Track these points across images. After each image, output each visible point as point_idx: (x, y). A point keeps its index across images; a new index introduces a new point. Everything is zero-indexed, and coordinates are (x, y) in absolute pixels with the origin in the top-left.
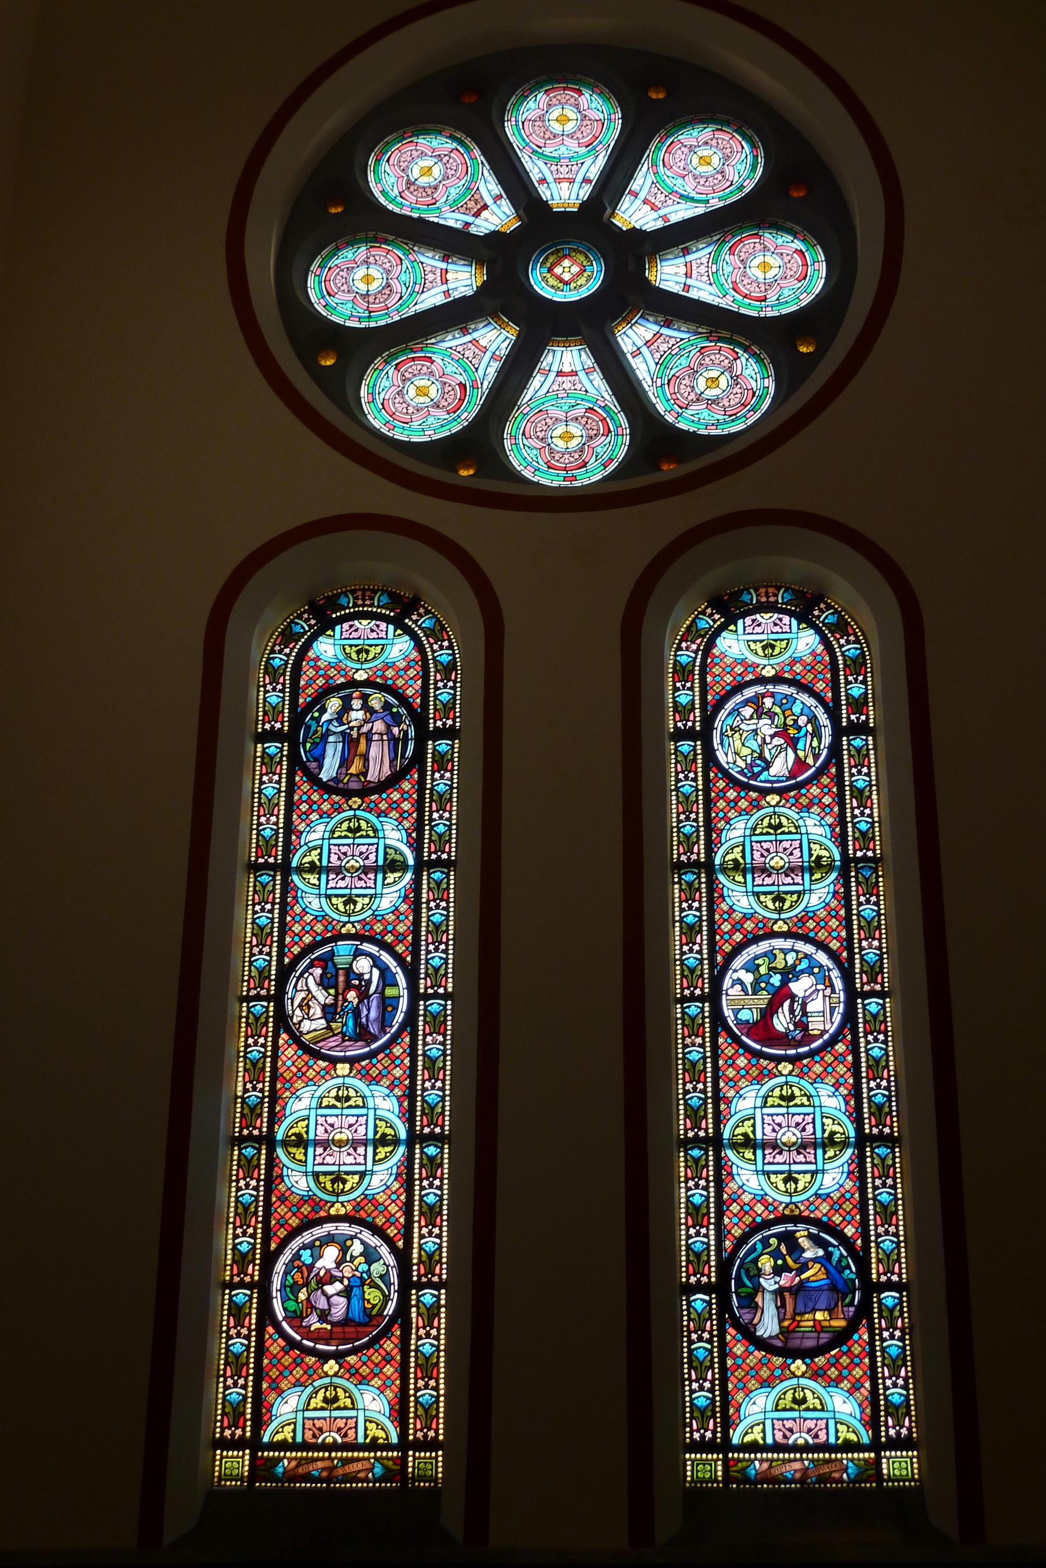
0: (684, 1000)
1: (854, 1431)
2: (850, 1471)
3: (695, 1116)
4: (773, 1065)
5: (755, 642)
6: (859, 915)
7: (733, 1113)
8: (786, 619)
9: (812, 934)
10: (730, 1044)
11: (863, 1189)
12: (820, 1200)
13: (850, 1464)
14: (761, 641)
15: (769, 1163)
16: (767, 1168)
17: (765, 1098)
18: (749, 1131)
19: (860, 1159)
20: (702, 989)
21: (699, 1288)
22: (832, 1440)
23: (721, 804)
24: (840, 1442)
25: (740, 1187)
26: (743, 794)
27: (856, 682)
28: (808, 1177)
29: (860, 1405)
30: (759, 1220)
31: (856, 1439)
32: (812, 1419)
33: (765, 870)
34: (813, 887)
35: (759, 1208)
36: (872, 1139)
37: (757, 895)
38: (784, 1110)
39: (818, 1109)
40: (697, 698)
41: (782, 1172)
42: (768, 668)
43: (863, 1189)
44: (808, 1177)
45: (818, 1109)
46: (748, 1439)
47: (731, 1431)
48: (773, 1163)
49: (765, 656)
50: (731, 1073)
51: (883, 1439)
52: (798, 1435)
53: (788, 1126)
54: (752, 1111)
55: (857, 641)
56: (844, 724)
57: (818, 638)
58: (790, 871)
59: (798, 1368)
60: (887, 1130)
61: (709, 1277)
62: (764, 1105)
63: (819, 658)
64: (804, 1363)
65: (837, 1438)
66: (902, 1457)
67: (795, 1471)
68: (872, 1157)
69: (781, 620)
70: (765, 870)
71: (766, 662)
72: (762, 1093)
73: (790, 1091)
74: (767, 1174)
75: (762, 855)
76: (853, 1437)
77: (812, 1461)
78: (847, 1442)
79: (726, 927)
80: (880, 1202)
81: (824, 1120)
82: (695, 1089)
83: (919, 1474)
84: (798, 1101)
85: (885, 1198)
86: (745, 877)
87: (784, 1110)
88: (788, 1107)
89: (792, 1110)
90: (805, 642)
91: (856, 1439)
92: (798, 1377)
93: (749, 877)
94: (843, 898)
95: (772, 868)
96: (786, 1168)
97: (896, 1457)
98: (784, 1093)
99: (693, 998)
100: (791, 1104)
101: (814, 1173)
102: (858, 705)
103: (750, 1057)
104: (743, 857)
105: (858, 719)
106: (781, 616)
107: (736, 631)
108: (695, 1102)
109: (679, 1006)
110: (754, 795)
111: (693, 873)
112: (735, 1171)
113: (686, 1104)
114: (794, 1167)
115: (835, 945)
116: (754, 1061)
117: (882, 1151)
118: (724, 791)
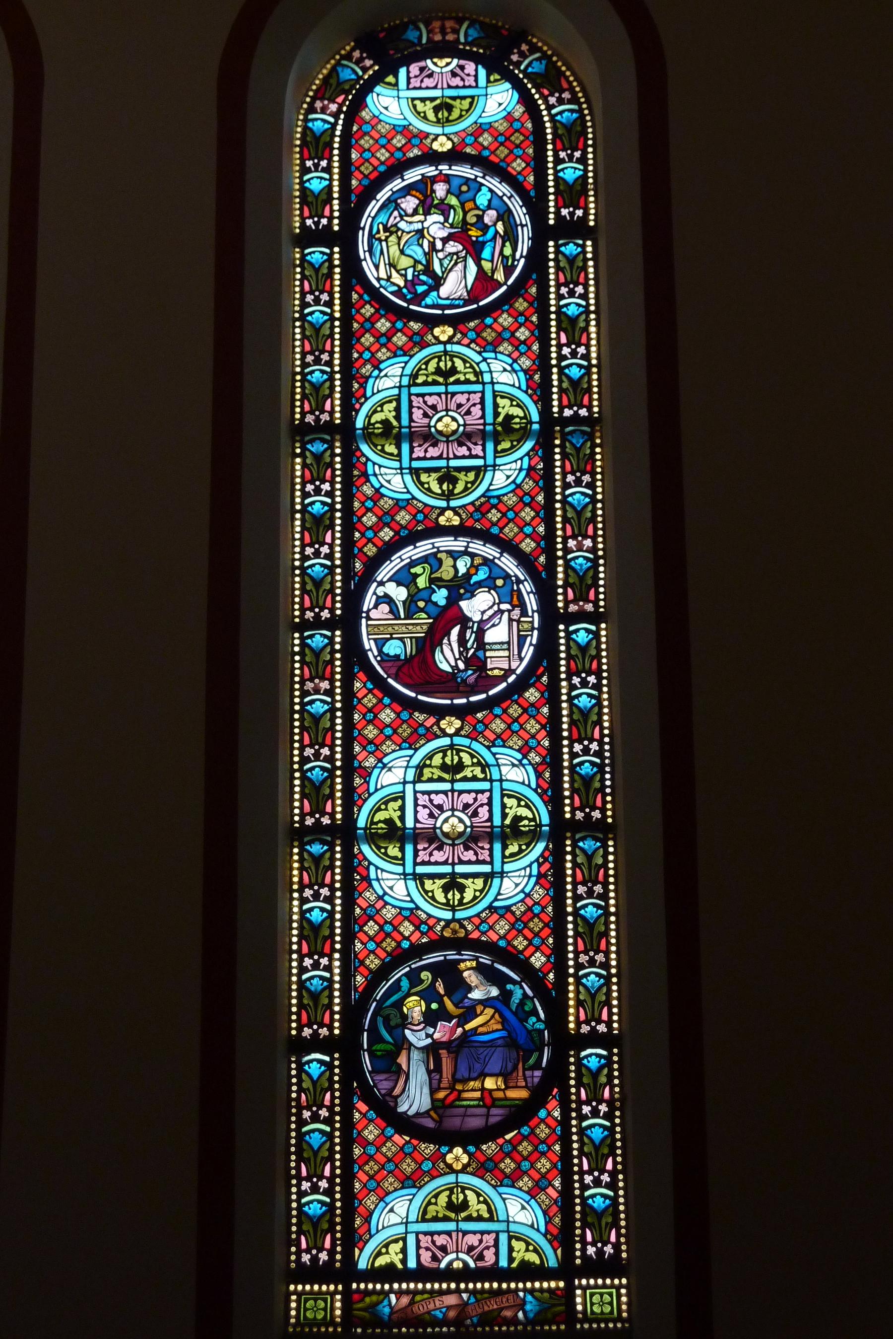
0: (305, 625)
1: (535, 1251)
2: (528, 1307)
3: (316, 794)
4: (432, 720)
5: (423, 100)
6: (564, 501)
7: (372, 790)
8: (470, 67)
9: (495, 530)
10: (370, 691)
11: (559, 900)
12: (495, 917)
13: (529, 1298)
14: (432, 99)
15: (423, 863)
16: (420, 870)
17: (420, 768)
18: (395, 816)
19: (556, 856)
20: (332, 610)
21: (316, 1044)
22: (503, 1263)
23: (368, 339)
24: (514, 1265)
25: (380, 898)
26: (399, 325)
27: (571, 160)
28: (479, 883)
29: (545, 1213)
30: (405, 944)
31: (538, 1262)
32: (474, 1233)
33: (429, 437)
34: (499, 461)
35: (407, 928)
36: (574, 826)
37: (415, 473)
38: (447, 786)
39: (496, 785)
40: (336, 183)
41: (441, 876)
42: (442, 139)
43: (559, 900)
44: (479, 883)
45: (496, 785)
46: (381, 1261)
47: (357, 1251)
48: (429, 863)
49: (438, 121)
50: (371, 732)
51: (578, 1261)
52: (454, 1256)
53: (453, 810)
54: (400, 788)
55: (574, 100)
56: (551, 222)
57: (516, 96)
58: (465, 437)
59: (457, 1159)
60: (596, 814)
61: (331, 1028)
62: (418, 779)
63: (517, 125)
64: (466, 1151)
65: (511, 1260)
66: (604, 1286)
67: (449, 1308)
68: (573, 853)
69: (462, 68)
70: (429, 437)
71: (438, 130)
72: (415, 761)
73: (456, 759)
74: (420, 879)
75: (425, 415)
76: (534, 1258)
77: (474, 1292)
78: (524, 1263)
79: (370, 520)
80: (583, 918)
81: (506, 800)
82: (317, 755)
83: (628, 1311)
84: (468, 773)
85: (590, 912)
86: (399, 447)
87: (447, 786)
88: (453, 781)
89: (458, 786)
90: (498, 101)
91: (538, 1262)
92: (457, 1172)
93: (405, 447)
94: (542, 477)
95: (440, 433)
96: (447, 869)
97: (596, 1286)
98: (448, 760)
99: (318, 623)
100: (458, 777)
101: (488, 877)
102: (572, 194)
103: (399, 709)
104: (398, 417)
105: (572, 214)
106: (462, 62)
107: (396, 84)
108: (317, 775)
109: (297, 635)
110: (415, 326)
111: (324, 441)
112: (373, 875)
113: (303, 778)
114: (459, 869)
115: (528, 545)
116: (405, 715)
117: (588, 845)
118: (373, 320)
